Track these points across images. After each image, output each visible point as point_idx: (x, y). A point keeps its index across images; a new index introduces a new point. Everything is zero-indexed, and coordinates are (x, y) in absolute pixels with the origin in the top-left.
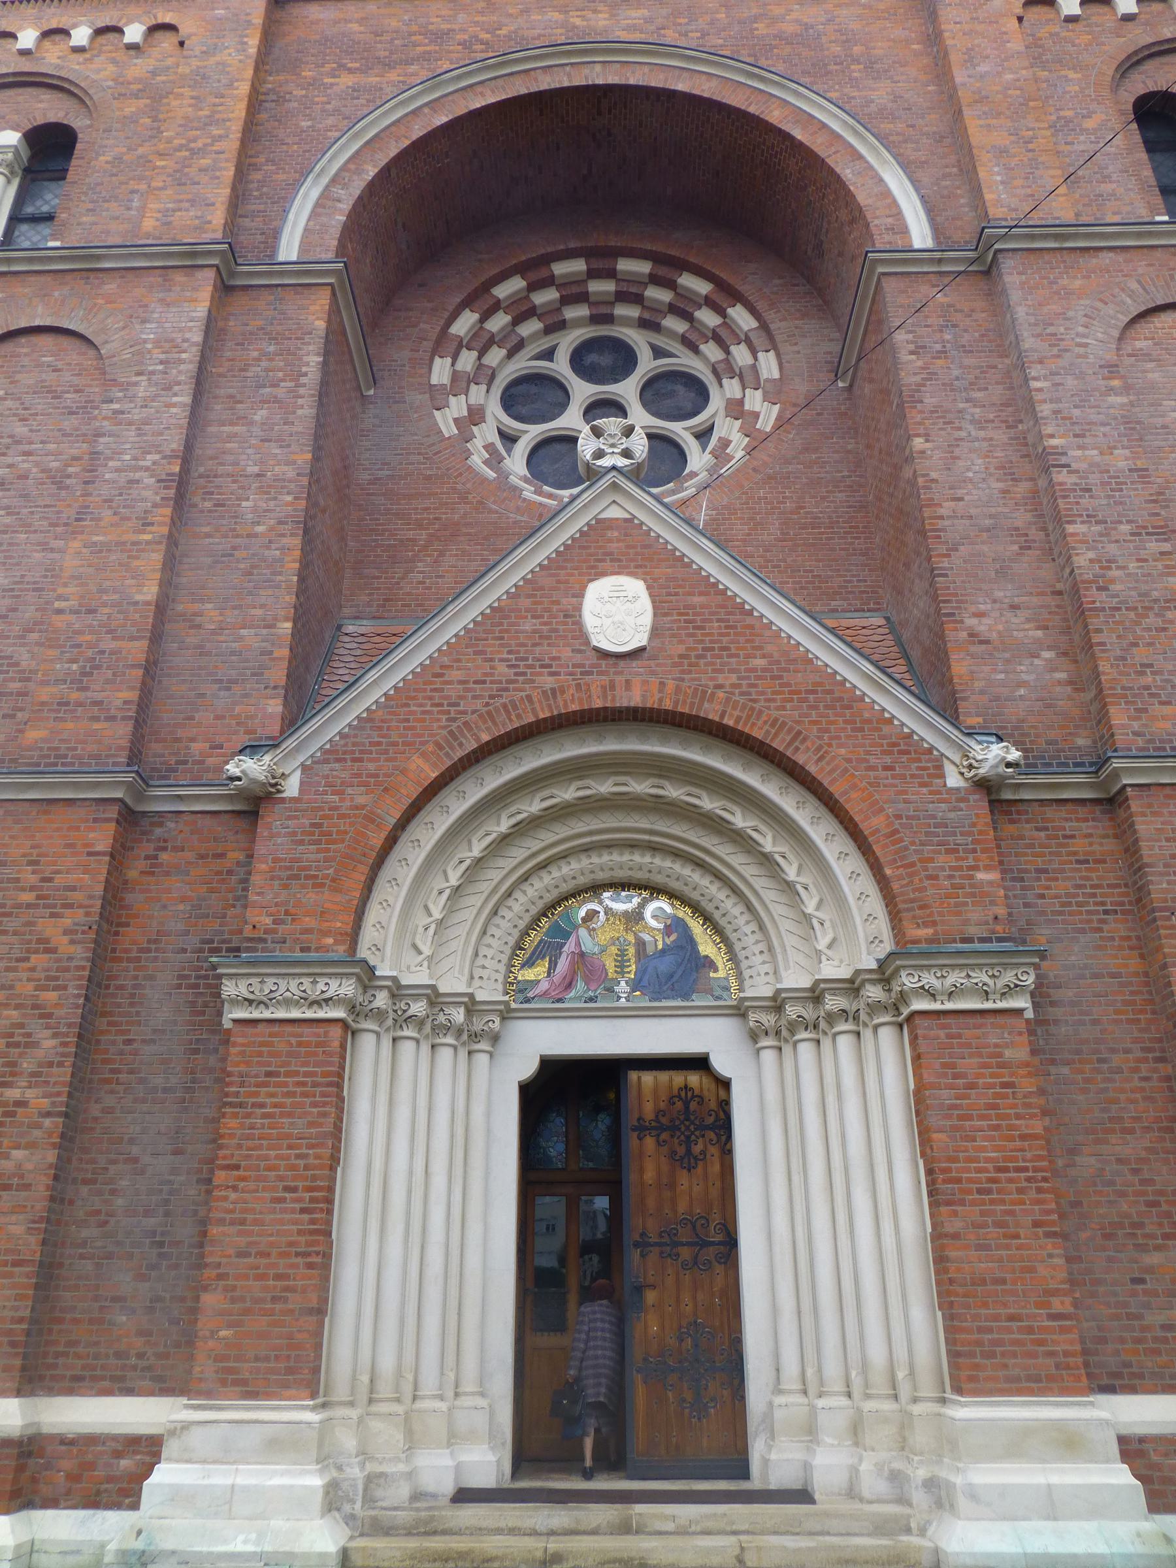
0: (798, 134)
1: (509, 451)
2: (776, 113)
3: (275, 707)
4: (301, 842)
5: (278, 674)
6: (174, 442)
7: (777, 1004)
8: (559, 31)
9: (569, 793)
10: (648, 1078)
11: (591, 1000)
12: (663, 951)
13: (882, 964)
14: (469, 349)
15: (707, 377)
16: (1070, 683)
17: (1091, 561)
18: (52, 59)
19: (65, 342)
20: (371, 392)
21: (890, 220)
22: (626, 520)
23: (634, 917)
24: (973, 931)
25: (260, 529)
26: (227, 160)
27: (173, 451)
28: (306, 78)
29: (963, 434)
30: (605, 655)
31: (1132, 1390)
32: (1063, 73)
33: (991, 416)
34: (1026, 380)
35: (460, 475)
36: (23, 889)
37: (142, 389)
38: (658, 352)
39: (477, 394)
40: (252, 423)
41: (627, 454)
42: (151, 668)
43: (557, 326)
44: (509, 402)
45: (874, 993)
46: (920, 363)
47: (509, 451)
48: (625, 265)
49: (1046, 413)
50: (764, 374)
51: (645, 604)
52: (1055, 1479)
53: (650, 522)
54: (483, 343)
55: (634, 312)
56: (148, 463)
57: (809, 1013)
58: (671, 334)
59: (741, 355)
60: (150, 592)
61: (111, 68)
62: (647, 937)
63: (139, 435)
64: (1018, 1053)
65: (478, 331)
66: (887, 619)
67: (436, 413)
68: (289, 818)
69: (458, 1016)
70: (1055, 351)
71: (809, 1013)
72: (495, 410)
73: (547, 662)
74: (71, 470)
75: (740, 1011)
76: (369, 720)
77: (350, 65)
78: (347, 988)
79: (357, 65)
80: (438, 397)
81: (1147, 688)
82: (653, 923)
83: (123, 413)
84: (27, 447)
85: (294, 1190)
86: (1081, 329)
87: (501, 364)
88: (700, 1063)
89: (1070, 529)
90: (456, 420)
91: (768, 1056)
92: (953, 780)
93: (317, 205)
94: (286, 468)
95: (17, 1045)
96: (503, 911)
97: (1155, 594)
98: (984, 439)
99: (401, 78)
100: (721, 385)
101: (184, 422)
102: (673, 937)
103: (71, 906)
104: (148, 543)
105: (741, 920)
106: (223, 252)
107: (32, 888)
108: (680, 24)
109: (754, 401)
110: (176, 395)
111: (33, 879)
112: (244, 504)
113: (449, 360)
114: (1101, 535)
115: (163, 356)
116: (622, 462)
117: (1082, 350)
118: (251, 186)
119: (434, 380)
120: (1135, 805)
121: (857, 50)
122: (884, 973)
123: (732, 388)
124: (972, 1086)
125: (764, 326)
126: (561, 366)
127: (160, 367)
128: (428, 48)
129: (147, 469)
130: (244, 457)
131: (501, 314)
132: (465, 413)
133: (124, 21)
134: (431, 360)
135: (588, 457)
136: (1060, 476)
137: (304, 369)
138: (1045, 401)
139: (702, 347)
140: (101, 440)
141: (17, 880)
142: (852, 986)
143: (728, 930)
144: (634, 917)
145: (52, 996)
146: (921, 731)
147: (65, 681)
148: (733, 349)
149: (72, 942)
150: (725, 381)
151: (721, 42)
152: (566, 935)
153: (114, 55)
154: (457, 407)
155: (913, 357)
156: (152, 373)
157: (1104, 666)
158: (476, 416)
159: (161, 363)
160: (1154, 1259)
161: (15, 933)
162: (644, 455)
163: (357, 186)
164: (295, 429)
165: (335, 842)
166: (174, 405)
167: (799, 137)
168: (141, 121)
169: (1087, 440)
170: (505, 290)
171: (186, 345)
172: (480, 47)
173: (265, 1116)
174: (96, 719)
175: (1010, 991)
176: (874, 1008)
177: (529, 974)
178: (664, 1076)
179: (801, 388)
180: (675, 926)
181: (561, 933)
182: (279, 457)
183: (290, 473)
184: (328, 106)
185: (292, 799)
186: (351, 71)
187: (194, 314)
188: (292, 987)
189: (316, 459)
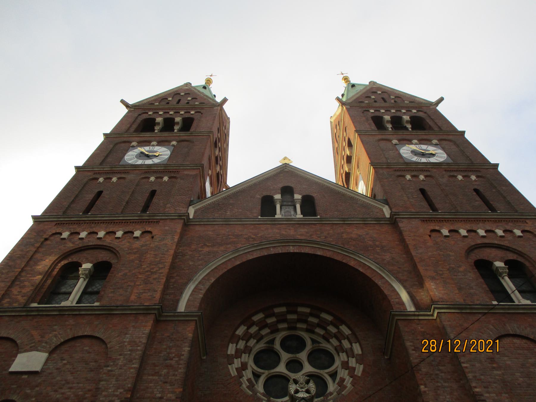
0: (361, 269)
8: (278, 235)
14: (242, 340)
15: (333, 352)
18: (109, 241)
20: (205, 358)
21: (397, 300)
26: (163, 276)
27: (129, 388)
28: (193, 248)
33: (449, 377)
34: (460, 363)
35: (238, 393)
37: (121, 361)
38: (314, 341)
39: (245, 357)
40: (160, 375)
41: (308, 391)
43: (275, 330)
44: (256, 361)
46: (417, 354)
47: (257, 381)
48: (300, 309)
49: (471, 377)
50: (356, 352)
54: (247, 337)
55: (304, 326)
56: (118, 393)
58: (319, 335)
59: (346, 344)
61: (128, 244)
63: (117, 381)
65: (246, 333)
67: (229, 366)
72: (251, 363)
74: (87, 395)
80: (230, 360)
83: (111, 371)
87: (254, 346)
90: (237, 369)
93: (193, 291)
94: (171, 395)
99: (225, 249)
100: (339, 355)
101: (135, 375)
106: (158, 309)
108: (318, 234)
109: (352, 362)
110: (133, 364)
113: (235, 344)
115: (130, 348)
116: (306, 395)
118: (170, 284)
119: (229, 353)
121: (377, 243)
123: (343, 356)
125: (354, 333)
126: (277, 346)
127: (129, 352)
128: (235, 240)
129: (117, 396)
130: (156, 390)
132: (240, 366)
133: (134, 230)
134: (228, 345)
135: (292, 393)
137: (183, 353)
139: (331, 340)
140: (102, 383)
148: (343, 341)
150: (340, 354)
151: (332, 239)
153: (129, 240)
154: (237, 363)
155: (414, 352)
156: (126, 355)
158: (244, 366)
159: (130, 350)
162: (315, 392)
163: (208, 285)
164: (177, 378)
166: (132, 368)
167: (361, 271)
168: (135, 262)
169: (490, 390)
170: (256, 318)
171: (140, 344)
182: (170, 390)
183: (174, 398)
184: (200, 258)
186: (208, 246)
187: (145, 332)
189: (184, 390)
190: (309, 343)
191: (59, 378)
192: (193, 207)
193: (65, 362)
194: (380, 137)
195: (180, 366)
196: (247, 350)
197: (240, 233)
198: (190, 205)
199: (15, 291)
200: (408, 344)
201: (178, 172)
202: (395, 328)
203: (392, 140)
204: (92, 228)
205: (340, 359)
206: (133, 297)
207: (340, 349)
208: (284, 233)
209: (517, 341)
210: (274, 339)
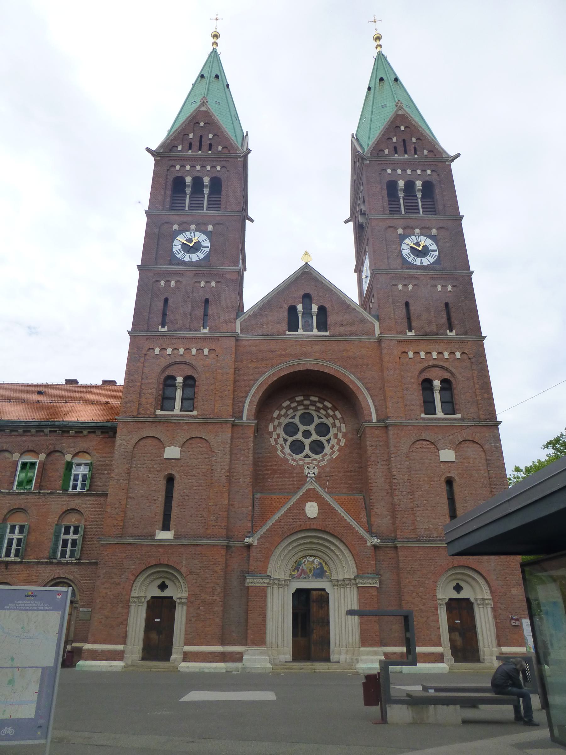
0: (351, 386)
1: (285, 443)
2: (347, 380)
4: (258, 554)
7: (337, 581)
9: (302, 542)
10: (315, 592)
11: (305, 578)
12: (318, 569)
13: (355, 577)
16: (392, 523)
17: (398, 500)
19: (201, 440)
20: (257, 434)
21: (368, 412)
22: (314, 489)
23: (313, 562)
24: (370, 572)
25: (244, 485)
29: (378, 467)
30: (309, 518)
31: (387, 646)
32: (407, 374)
36: (211, 562)
40: (240, 460)
41: (314, 473)
43: (295, 409)
45: (353, 582)
46: (371, 450)
47: (285, 443)
51: (317, 508)
52: (373, 658)
53: (318, 490)
55: (314, 408)
57: (342, 583)
60: (226, 502)
62: (315, 566)
64: (375, 593)
66: (364, 496)
68: (256, 549)
69: (283, 583)
70: (397, 451)
71: (342, 583)
72: (283, 434)
73: (299, 519)
75: (331, 581)
76: (268, 530)
77: (254, 360)
78: (268, 581)
79: (256, 360)
80: (270, 434)
81: (404, 527)
82: (316, 563)
84: (199, 467)
85: (260, 614)
86: (402, 445)
89: (395, 493)
91: (336, 590)
92: (369, 544)
95: (214, 590)
96: (290, 562)
97: (408, 507)
98: (382, 469)
99: (265, 365)
101: (229, 463)
102: (320, 566)
103: (219, 565)
104: (225, 491)
105: (332, 564)
107: (213, 561)
109: (340, 436)
110: (226, 456)
111: (212, 560)
112: (240, 479)
114: (400, 494)
115: (223, 446)
117: (401, 451)
120: (399, 550)
122: (355, 579)
124: (367, 599)
126: (297, 421)
127: (223, 449)
129: (223, 474)
131: (284, 409)
136: (395, 481)
137: (250, 447)
138: (393, 463)
140: (213, 466)
141: (210, 560)
142: (350, 580)
143: (329, 566)
144: (313, 562)
145: (218, 581)
146: (364, 535)
147: (213, 521)
149: (221, 571)
152: (300, 565)
156: (221, 450)
157: (397, 522)
159: (223, 448)
160: (393, 627)
161: (211, 570)
165: (263, 554)
166: (226, 458)
167: (351, 387)
172: (282, 356)
173: (256, 602)
174: (219, 528)
175: (374, 583)
176: (353, 584)
177: (293, 573)
178: (317, 592)
179: (350, 436)
180: (320, 564)
181: (299, 565)
185: (256, 545)
186: (254, 362)
188: (258, 580)
190: (316, 418)
191: (190, 462)
192: (239, 320)
193: (191, 453)
194: (389, 223)
195: (250, 455)
196: (280, 424)
198: (237, 319)
200: (368, 443)
201: (222, 275)
202: (363, 432)
203: (398, 229)
205: (333, 431)
207: (334, 425)
208: (304, 349)
209: (424, 443)
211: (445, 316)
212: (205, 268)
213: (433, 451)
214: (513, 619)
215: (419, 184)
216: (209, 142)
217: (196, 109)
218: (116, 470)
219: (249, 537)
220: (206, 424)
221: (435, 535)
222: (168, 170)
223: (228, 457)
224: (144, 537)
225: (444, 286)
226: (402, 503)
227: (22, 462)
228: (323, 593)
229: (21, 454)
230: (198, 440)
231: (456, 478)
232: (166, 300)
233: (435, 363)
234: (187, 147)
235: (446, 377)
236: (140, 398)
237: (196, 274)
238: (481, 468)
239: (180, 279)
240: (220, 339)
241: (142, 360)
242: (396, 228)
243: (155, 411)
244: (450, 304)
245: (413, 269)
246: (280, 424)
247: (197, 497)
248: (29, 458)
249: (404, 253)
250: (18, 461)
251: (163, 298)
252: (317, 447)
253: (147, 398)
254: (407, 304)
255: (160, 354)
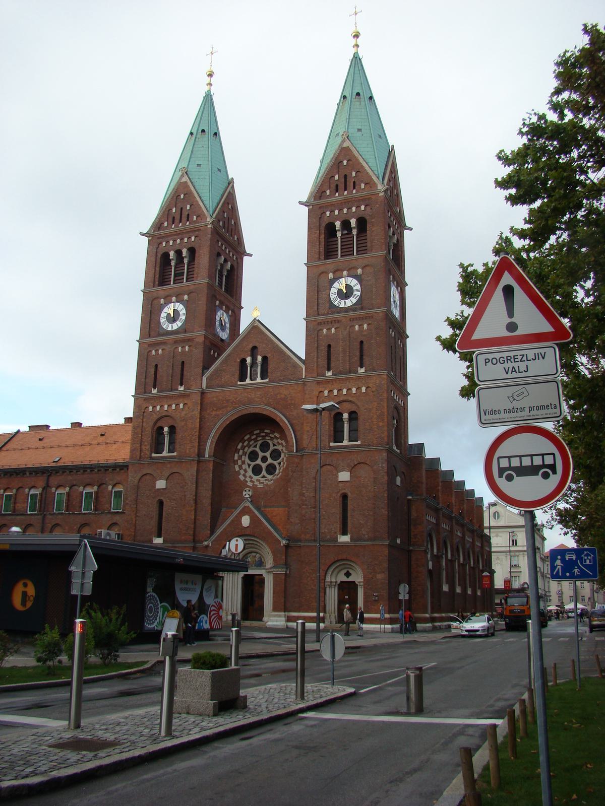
3: (209, 532)
5: (209, 528)
6: (194, 494)
10: (257, 577)
38: (274, 445)
41: (249, 495)
42: (195, 528)
60: (193, 517)
61: (179, 414)
72: (247, 461)
88: (262, 575)
92: (282, 545)
93: (211, 443)
126: (257, 449)
163: (216, 438)
175: (283, 571)
180: (260, 558)
186: (214, 410)
190: (271, 445)
191: (172, 491)
194: (322, 269)
197: (229, 398)
199: (143, 447)
204: (161, 402)
206: (188, 452)
208: (249, 396)
209: (329, 467)
210: (257, 445)
211: (358, 354)
212: (181, 336)
213: (335, 473)
214: (374, 596)
215: (353, 222)
216: (187, 213)
217: (178, 182)
218: (129, 498)
219: (206, 541)
220: (181, 462)
221: (328, 537)
222: (157, 248)
223: (195, 486)
224: (146, 542)
225: (361, 326)
226: (307, 514)
227: (85, 492)
228: (260, 577)
229: (84, 487)
230: (176, 474)
231: (349, 494)
232: (156, 366)
233: (345, 398)
234: (171, 223)
235: (353, 410)
236: (141, 446)
237: (176, 342)
238: (369, 485)
239: (164, 347)
240: (191, 395)
241: (141, 417)
242: (327, 273)
243: (151, 455)
244: (364, 342)
245: (338, 313)
246: (245, 454)
247: (176, 514)
248: (88, 490)
249: (332, 297)
250: (83, 492)
251: (154, 365)
252: (271, 469)
253: (145, 446)
254: (329, 346)
255: (153, 411)
